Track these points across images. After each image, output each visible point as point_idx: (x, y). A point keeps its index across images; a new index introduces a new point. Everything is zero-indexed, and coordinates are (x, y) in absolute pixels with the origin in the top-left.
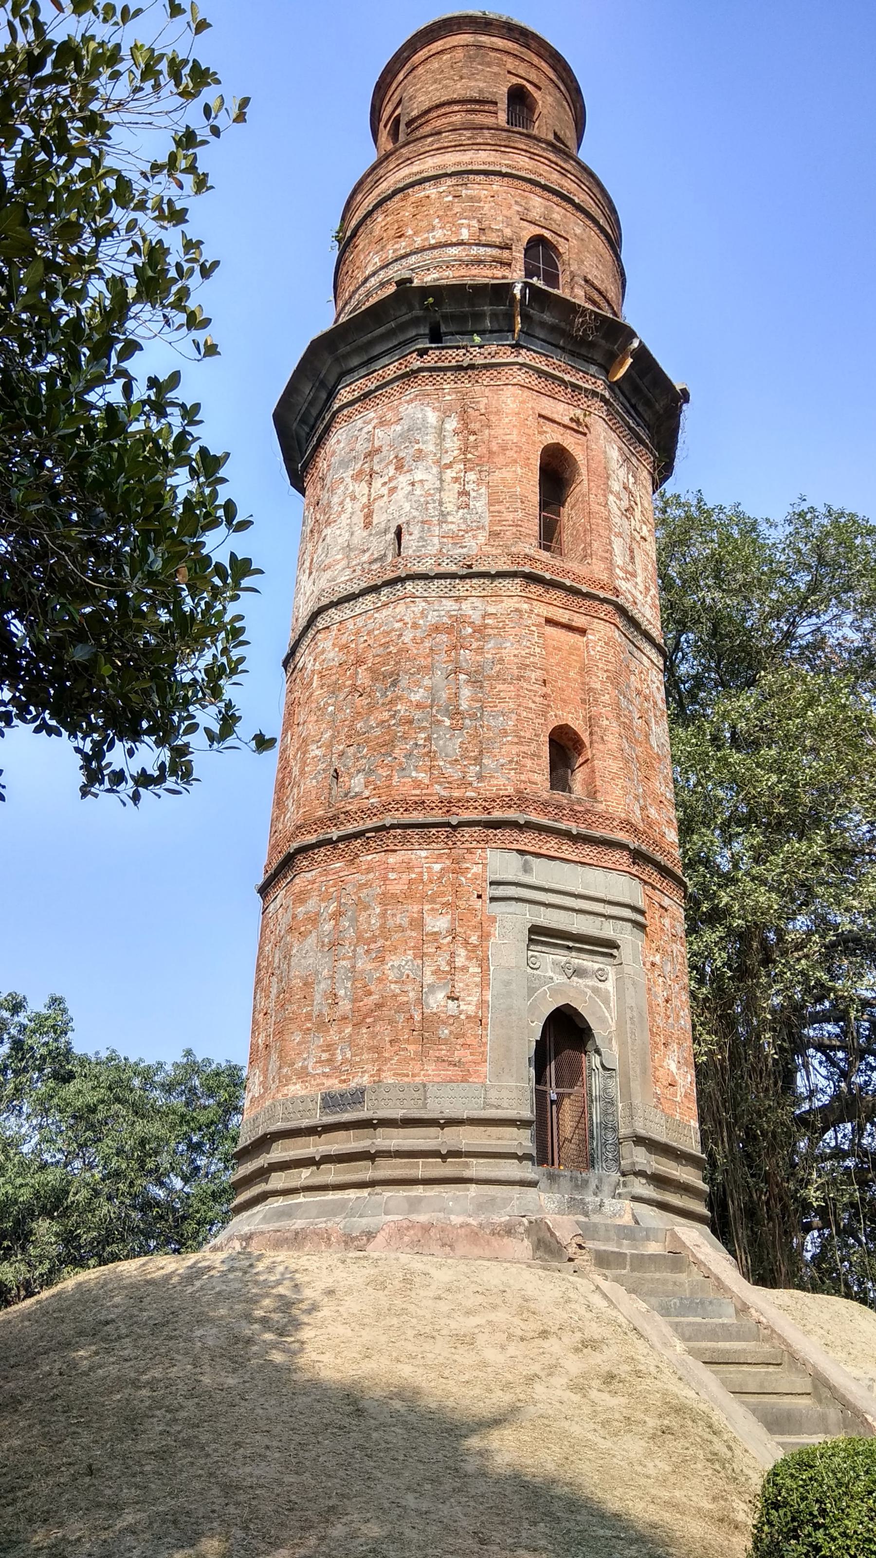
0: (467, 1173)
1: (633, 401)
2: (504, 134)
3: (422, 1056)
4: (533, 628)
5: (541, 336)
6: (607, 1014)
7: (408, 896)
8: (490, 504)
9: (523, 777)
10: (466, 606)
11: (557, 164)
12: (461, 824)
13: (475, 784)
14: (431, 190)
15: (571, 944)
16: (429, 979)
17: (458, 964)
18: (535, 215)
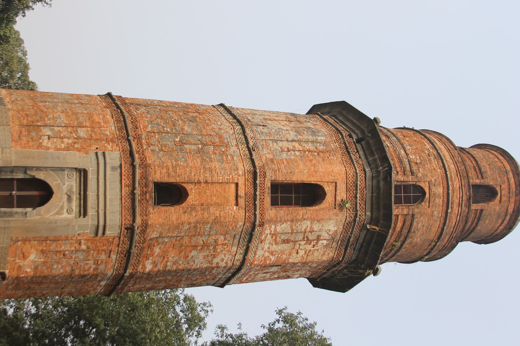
1: (364, 244)
2: (465, 175)
3: (22, 125)
4: (231, 176)
5: (374, 184)
6: (52, 213)
7: (93, 122)
9: (156, 167)
10: (234, 148)
11: (462, 201)
12: (129, 141)
13: (149, 148)
14: (428, 146)
15: (82, 193)
16: (56, 129)
17: (64, 140)
18: (433, 189)
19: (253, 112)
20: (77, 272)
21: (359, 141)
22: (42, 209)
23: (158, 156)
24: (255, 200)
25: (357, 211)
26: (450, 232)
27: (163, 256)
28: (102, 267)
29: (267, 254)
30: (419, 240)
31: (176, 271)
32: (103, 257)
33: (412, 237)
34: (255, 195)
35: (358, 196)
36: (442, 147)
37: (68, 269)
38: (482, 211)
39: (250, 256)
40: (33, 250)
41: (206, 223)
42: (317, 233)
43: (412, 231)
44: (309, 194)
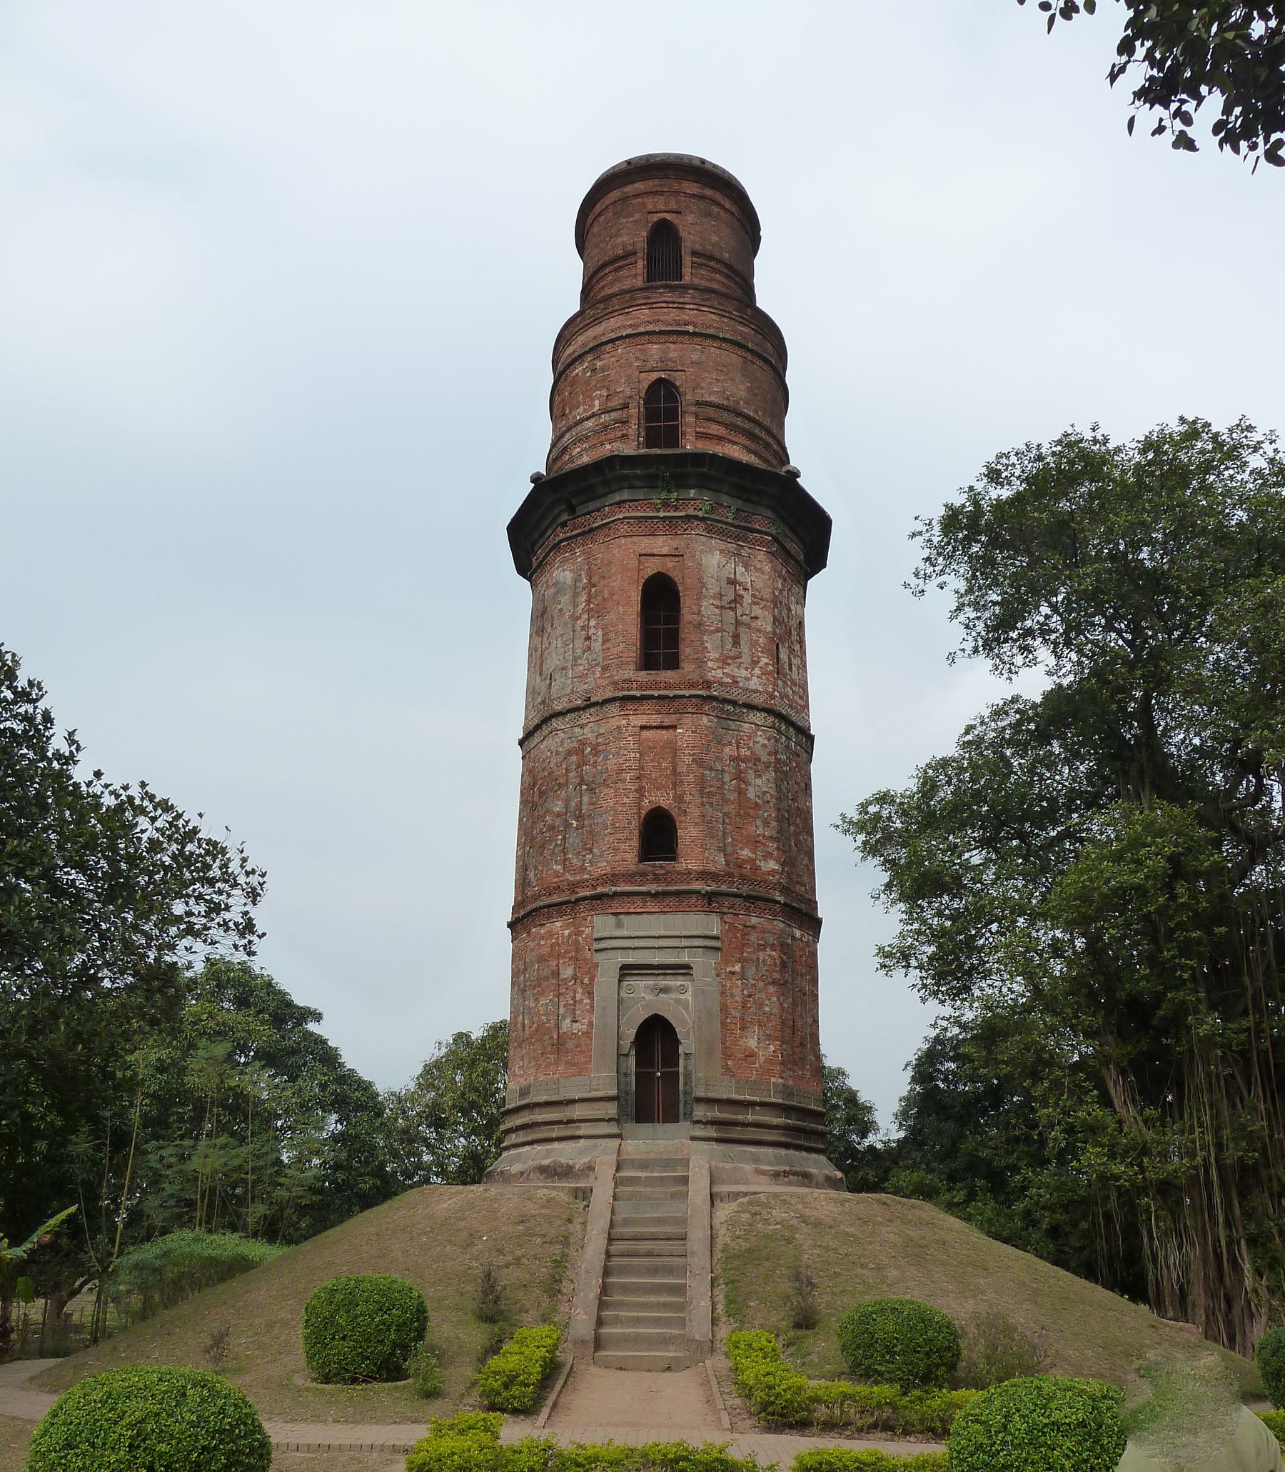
0: (580, 1133)
7: (551, 955)
8: (603, 643)
9: (617, 858)
12: (577, 900)
16: (562, 1011)
19: (532, 692)
20: (776, 976)
21: (572, 510)
22: (680, 1031)
23: (601, 856)
24: (667, 697)
25: (688, 517)
26: (732, 323)
27: (755, 843)
28: (771, 939)
29: (757, 671)
30: (742, 387)
31: (778, 820)
32: (753, 938)
33: (737, 402)
34: (660, 697)
35: (662, 514)
36: (580, 339)
37: (772, 989)
38: (694, 253)
39: (759, 700)
43: (725, 403)
44: (661, 599)
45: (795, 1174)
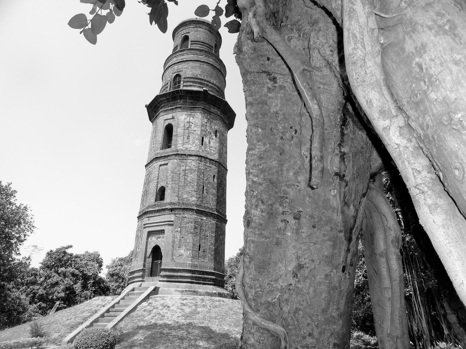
29: (194, 145)
32: (185, 220)
33: (197, 75)
35: (170, 108)
37: (190, 235)
40: (178, 251)
41: (173, 177)
42: (186, 123)
45: (191, 291)
